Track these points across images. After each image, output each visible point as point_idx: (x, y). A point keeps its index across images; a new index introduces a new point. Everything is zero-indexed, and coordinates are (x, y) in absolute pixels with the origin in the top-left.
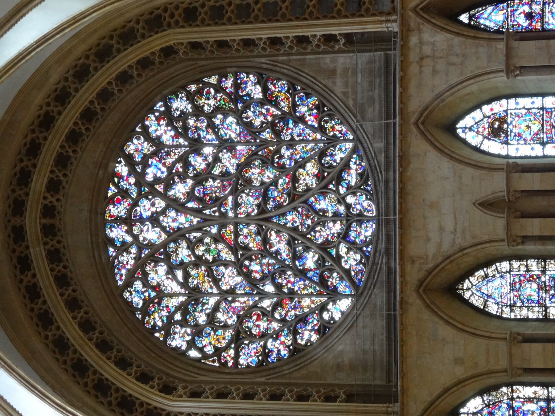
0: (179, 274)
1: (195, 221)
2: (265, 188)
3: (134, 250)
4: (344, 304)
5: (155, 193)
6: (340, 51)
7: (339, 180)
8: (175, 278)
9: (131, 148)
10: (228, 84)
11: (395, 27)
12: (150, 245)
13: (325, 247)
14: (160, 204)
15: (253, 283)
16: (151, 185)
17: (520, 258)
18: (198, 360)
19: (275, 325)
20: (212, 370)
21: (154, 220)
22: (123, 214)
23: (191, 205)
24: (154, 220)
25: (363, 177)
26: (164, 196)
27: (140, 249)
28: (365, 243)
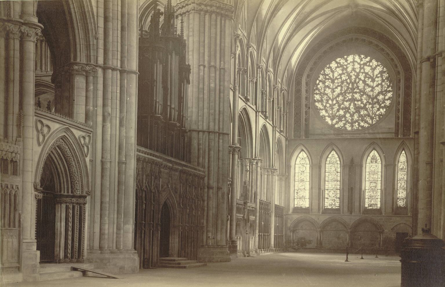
0: (339, 77)
1: (353, 81)
2: (361, 100)
3: (346, 63)
4: (330, 122)
5: (361, 68)
6: (396, 120)
7: (362, 121)
8: (338, 76)
9: (374, 61)
10: (390, 89)
11: (399, 136)
12: (347, 68)
13: (344, 116)
14: (358, 70)
15: (336, 98)
16: (363, 68)
17: (341, 166)
18: (316, 83)
19: (325, 104)
20: (313, 88)
21: (354, 69)
22: (355, 60)
23: (357, 80)
24: (354, 69)
25: (362, 127)
26: (360, 72)
27: (346, 65)
28: (346, 128)
